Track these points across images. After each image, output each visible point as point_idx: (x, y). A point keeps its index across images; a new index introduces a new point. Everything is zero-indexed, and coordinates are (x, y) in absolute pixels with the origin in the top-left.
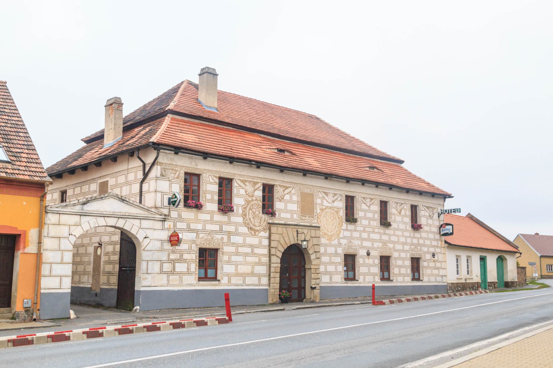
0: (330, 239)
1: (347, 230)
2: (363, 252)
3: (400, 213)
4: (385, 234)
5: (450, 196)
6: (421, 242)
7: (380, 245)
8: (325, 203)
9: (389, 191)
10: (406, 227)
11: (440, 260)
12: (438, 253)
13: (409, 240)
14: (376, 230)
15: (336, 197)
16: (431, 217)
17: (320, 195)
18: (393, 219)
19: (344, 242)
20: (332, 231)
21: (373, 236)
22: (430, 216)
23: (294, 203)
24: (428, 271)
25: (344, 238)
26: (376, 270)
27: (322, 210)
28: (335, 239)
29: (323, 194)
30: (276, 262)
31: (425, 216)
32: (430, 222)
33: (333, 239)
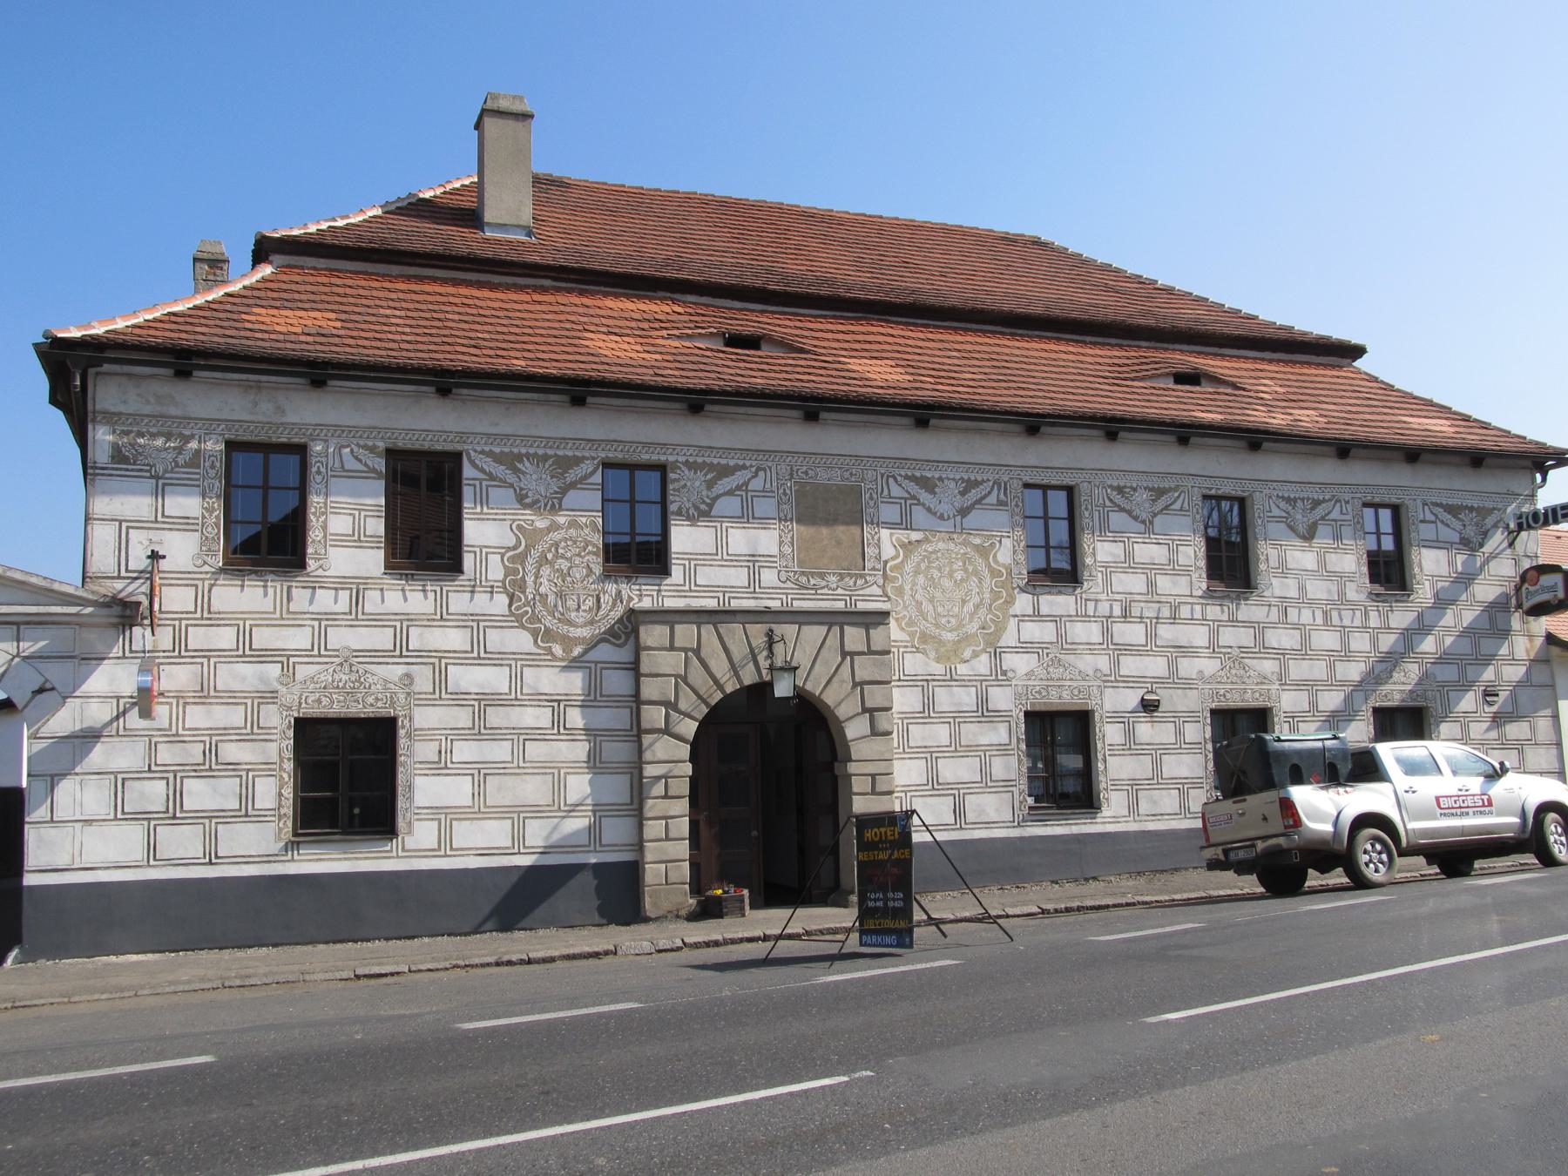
1: (1037, 616)
4: (1233, 621)
7: (1210, 666)
15: (974, 494)
17: (896, 491)
18: (1273, 562)
19: (1020, 664)
20: (960, 625)
25: (1025, 647)
28: (975, 655)
29: (913, 488)
33: (967, 654)
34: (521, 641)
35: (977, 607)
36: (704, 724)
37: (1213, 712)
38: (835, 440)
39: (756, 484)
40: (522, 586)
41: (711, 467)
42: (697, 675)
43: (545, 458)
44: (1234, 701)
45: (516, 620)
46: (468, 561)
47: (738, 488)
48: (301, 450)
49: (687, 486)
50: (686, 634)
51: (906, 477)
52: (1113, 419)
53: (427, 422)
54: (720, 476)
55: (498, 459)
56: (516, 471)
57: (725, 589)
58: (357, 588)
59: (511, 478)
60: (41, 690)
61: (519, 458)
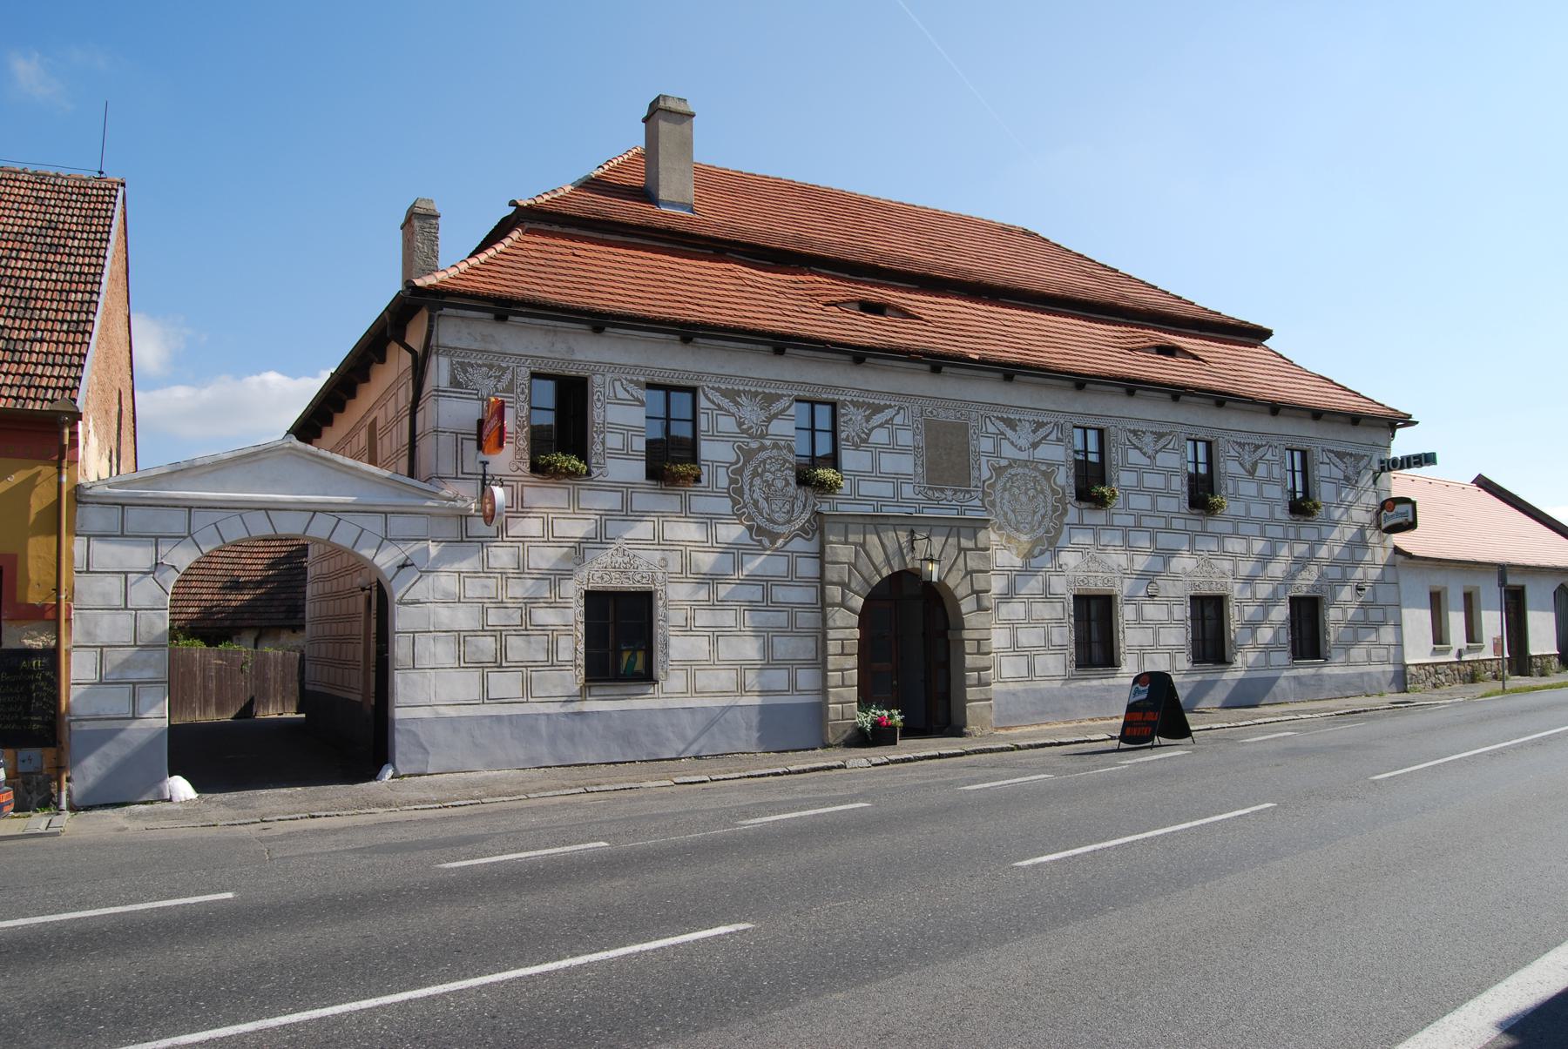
9: (1216, 411)
10: (1272, 513)
15: (1042, 432)
17: (991, 429)
18: (1230, 490)
22: (1347, 478)
23: (903, 451)
27: (999, 471)
29: (1002, 426)
31: (1331, 479)
35: (1043, 517)
36: (868, 600)
37: (1192, 598)
38: (949, 387)
39: (898, 420)
40: (740, 492)
41: (869, 405)
43: (756, 394)
45: (738, 515)
47: (887, 422)
52: (1135, 381)
54: (873, 414)
55: (725, 393)
56: (737, 403)
58: (625, 489)
59: (733, 409)
61: (738, 393)
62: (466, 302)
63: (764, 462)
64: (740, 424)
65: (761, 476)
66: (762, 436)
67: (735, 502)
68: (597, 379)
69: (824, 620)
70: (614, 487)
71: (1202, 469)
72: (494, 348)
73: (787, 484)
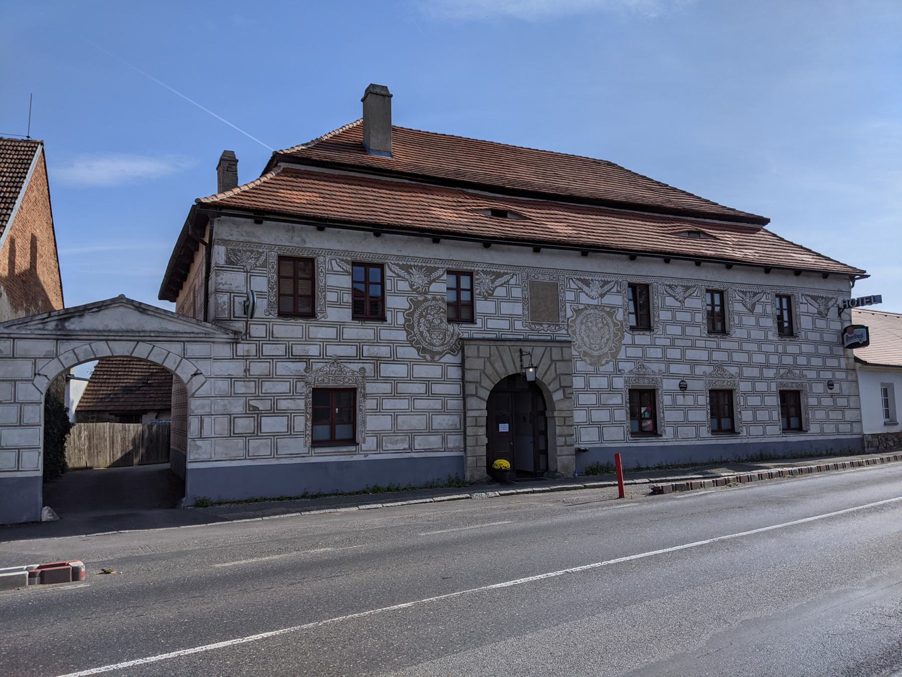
0: (596, 362)
1: (633, 345)
2: (670, 385)
3: (752, 310)
4: (718, 349)
5: (863, 275)
6: (802, 361)
7: (709, 369)
8: (584, 299)
9: (726, 271)
10: (766, 336)
11: (846, 392)
12: (841, 380)
13: (774, 360)
14: (700, 344)
15: (607, 288)
16: (822, 315)
17: (573, 286)
18: (737, 322)
19: (627, 367)
20: (600, 349)
21: (691, 354)
22: (820, 313)
23: (516, 300)
24: (820, 415)
25: (628, 359)
26: (702, 415)
27: (578, 311)
28: (607, 362)
29: (580, 284)
30: (478, 408)
31: (807, 314)
32: (821, 324)
33: (603, 362)
34: (411, 353)
35: (608, 340)
38: (548, 261)
39: (513, 281)
42: (489, 370)
43: (422, 267)
44: (718, 386)
45: (411, 342)
46: (388, 315)
47: (505, 283)
48: (312, 260)
49: (483, 283)
50: (484, 350)
51: (577, 279)
52: (669, 253)
53: (370, 248)
55: (402, 267)
56: (409, 273)
57: (499, 330)
58: (339, 326)
59: (407, 277)
60: (195, 374)
61: (411, 267)
62: (236, 212)
63: (427, 308)
64: (411, 286)
65: (425, 317)
66: (426, 293)
67: (408, 333)
68: (321, 259)
69: (464, 405)
70: (332, 325)
71: (717, 309)
72: (255, 240)
73: (442, 322)
